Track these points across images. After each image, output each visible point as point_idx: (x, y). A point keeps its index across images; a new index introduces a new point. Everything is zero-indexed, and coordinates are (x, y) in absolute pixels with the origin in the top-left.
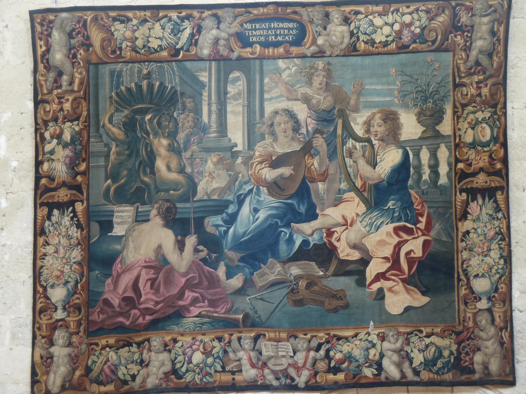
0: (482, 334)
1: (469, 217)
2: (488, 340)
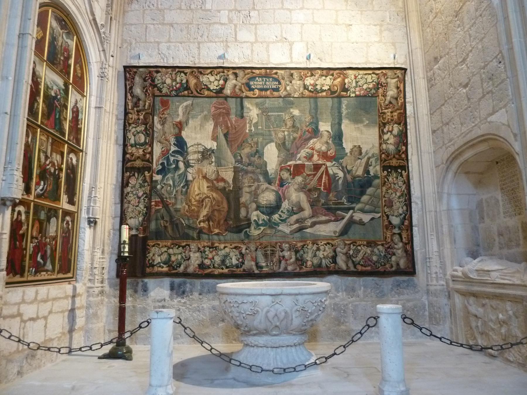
0: (396, 246)
2: (398, 249)
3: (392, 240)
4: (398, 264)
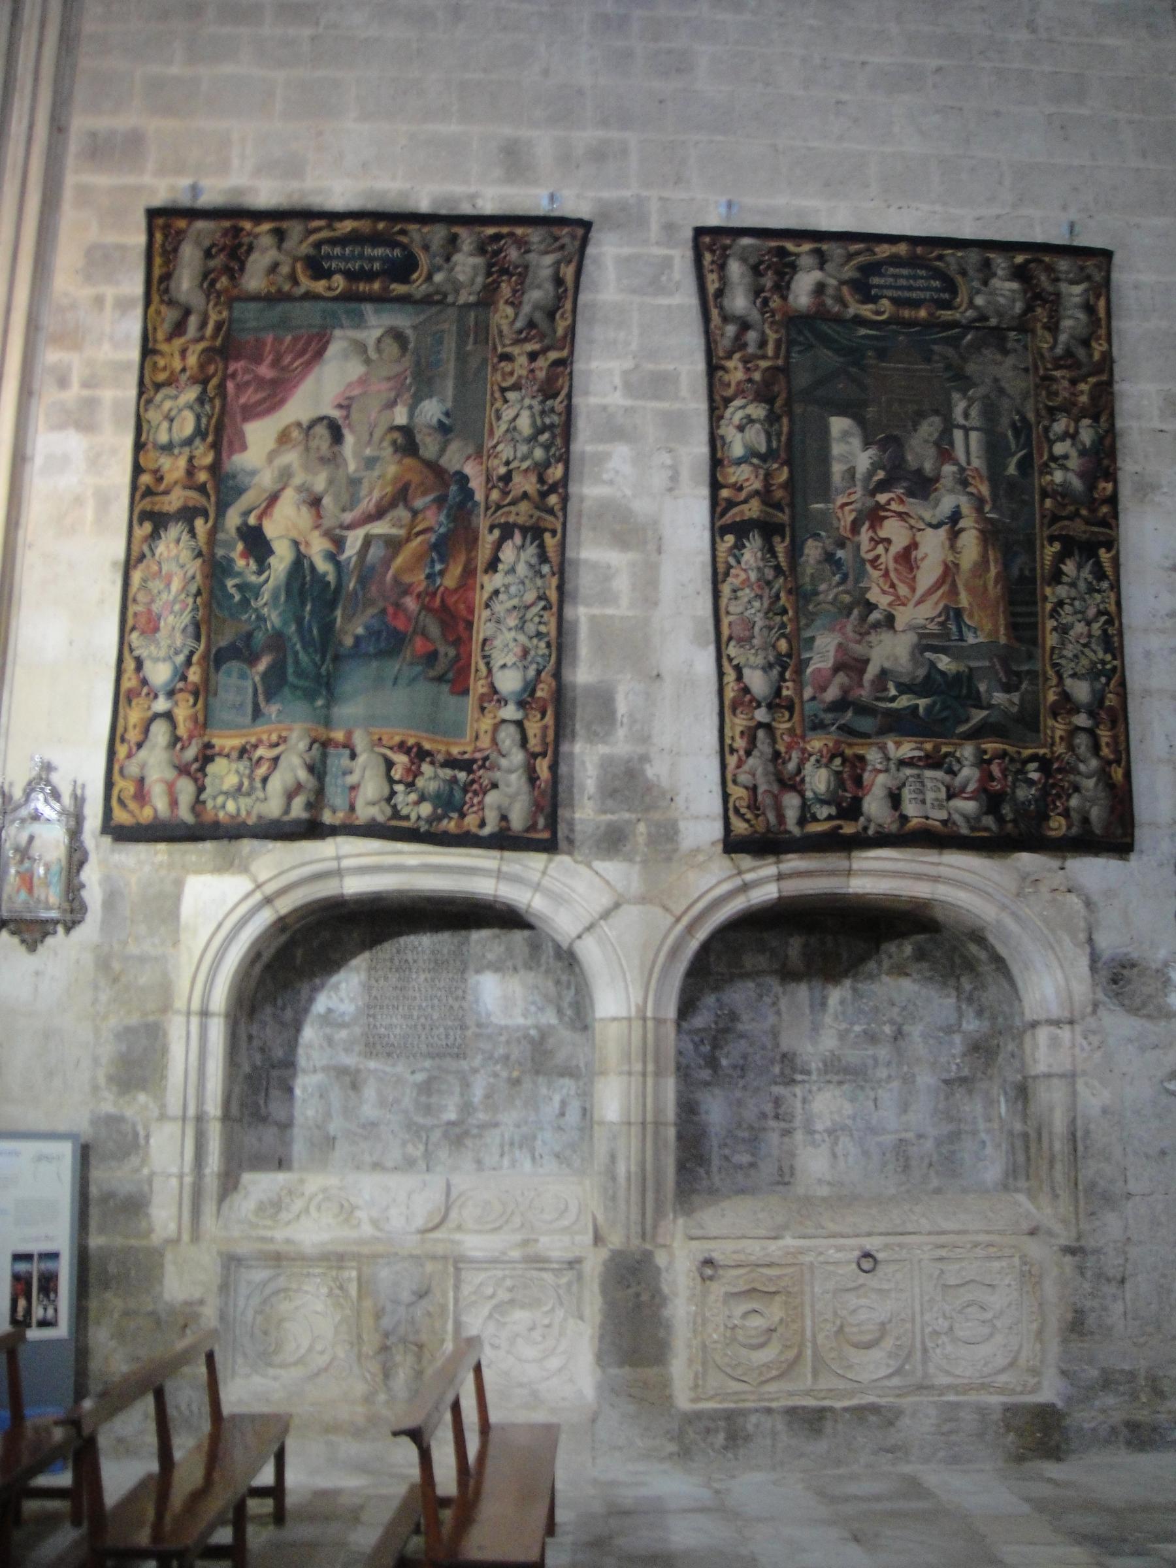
0: (504, 762)
1: (500, 567)
2: (510, 771)
3: (494, 741)
4: (504, 818)
